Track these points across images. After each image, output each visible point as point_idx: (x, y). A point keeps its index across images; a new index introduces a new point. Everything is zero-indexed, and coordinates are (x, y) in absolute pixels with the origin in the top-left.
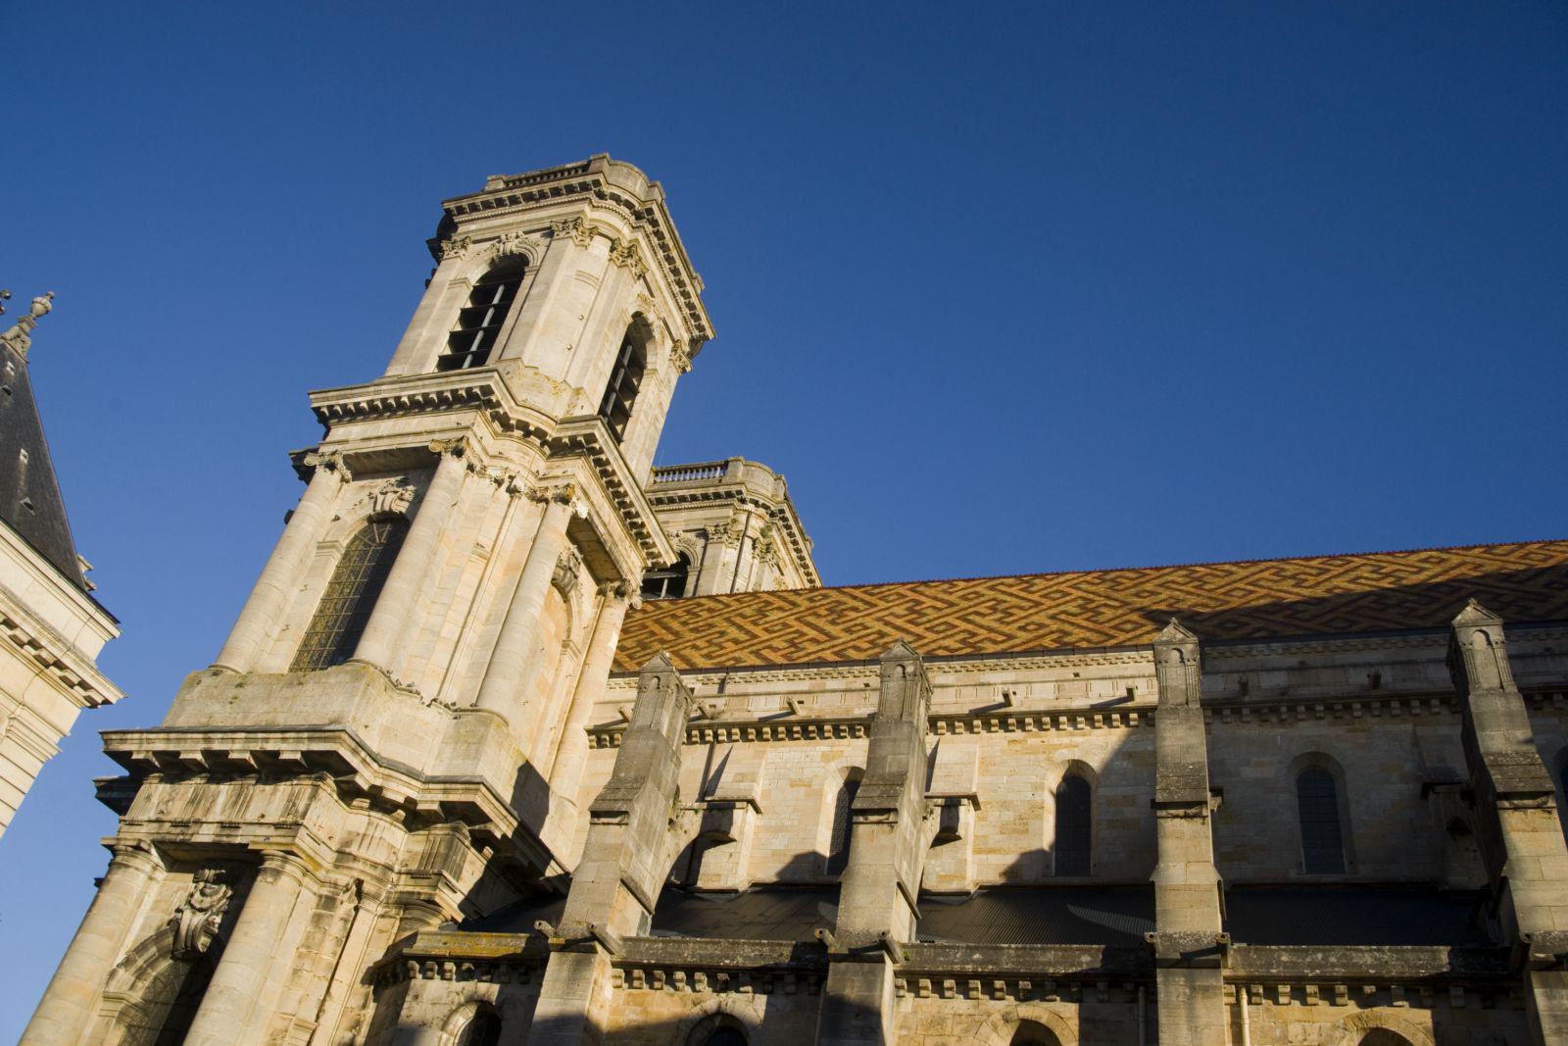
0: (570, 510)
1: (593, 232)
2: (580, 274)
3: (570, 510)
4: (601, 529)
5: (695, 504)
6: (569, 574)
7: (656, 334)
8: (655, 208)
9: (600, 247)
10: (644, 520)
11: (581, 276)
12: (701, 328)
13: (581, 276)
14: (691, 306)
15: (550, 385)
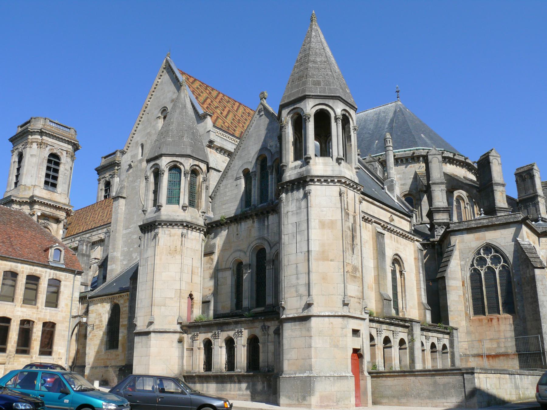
0: (36, 215)
1: (32, 142)
2: (31, 155)
3: (36, 215)
4: (48, 213)
5: (109, 167)
6: (45, 224)
7: (59, 154)
8: (43, 130)
9: (35, 145)
10: (58, 205)
11: (32, 156)
12: (74, 143)
13: (32, 156)
14: (68, 141)
15: (28, 188)
